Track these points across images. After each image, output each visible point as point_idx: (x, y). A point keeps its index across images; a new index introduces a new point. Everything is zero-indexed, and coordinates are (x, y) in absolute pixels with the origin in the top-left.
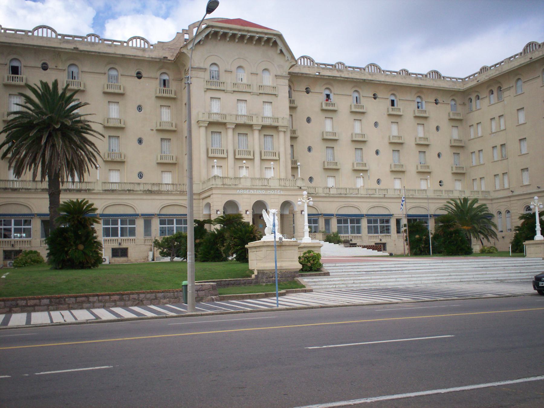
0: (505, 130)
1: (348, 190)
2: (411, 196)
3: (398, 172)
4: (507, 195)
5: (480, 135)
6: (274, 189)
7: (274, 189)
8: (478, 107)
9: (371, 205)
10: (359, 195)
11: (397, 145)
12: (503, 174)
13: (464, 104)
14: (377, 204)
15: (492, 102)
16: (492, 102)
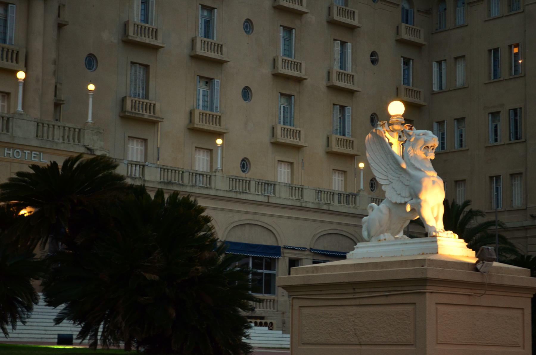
0: (524, 76)
1: (186, 175)
2: (325, 207)
3: (286, 148)
4: (518, 224)
5: (460, 81)
6: (23, 147)
7: (23, 147)
8: (460, 21)
9: (237, 218)
10: (212, 192)
11: (288, 83)
12: (512, 175)
13: (428, 12)
14: (250, 217)
15: (495, 13)
16: (495, 13)
